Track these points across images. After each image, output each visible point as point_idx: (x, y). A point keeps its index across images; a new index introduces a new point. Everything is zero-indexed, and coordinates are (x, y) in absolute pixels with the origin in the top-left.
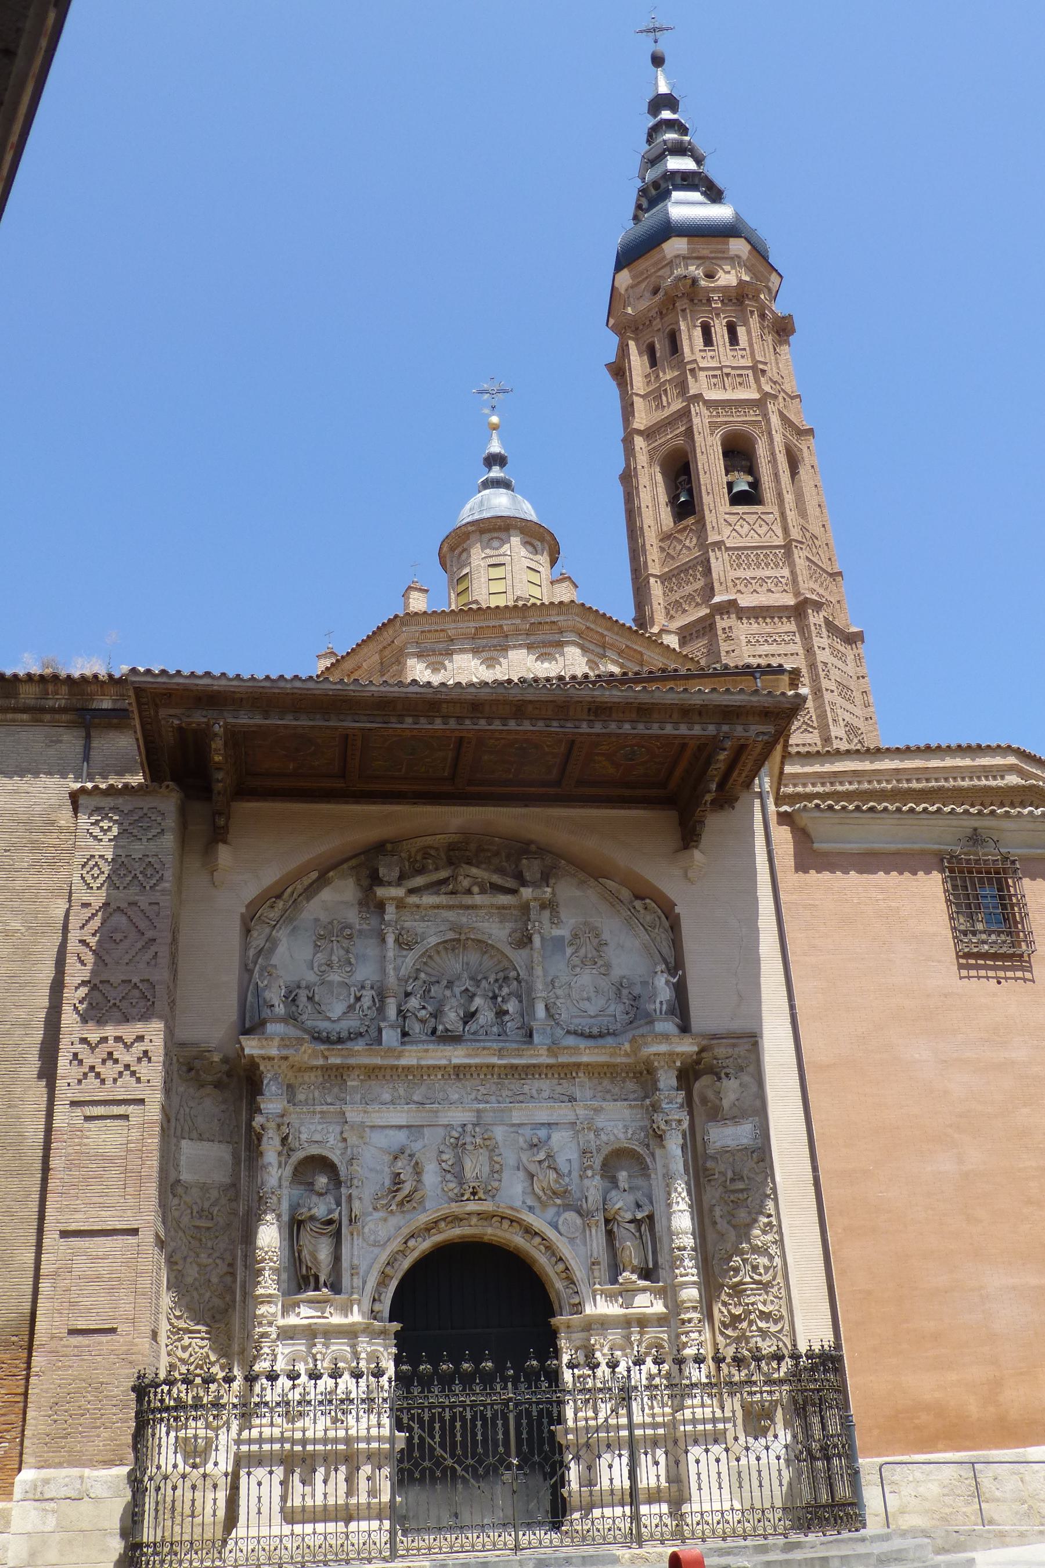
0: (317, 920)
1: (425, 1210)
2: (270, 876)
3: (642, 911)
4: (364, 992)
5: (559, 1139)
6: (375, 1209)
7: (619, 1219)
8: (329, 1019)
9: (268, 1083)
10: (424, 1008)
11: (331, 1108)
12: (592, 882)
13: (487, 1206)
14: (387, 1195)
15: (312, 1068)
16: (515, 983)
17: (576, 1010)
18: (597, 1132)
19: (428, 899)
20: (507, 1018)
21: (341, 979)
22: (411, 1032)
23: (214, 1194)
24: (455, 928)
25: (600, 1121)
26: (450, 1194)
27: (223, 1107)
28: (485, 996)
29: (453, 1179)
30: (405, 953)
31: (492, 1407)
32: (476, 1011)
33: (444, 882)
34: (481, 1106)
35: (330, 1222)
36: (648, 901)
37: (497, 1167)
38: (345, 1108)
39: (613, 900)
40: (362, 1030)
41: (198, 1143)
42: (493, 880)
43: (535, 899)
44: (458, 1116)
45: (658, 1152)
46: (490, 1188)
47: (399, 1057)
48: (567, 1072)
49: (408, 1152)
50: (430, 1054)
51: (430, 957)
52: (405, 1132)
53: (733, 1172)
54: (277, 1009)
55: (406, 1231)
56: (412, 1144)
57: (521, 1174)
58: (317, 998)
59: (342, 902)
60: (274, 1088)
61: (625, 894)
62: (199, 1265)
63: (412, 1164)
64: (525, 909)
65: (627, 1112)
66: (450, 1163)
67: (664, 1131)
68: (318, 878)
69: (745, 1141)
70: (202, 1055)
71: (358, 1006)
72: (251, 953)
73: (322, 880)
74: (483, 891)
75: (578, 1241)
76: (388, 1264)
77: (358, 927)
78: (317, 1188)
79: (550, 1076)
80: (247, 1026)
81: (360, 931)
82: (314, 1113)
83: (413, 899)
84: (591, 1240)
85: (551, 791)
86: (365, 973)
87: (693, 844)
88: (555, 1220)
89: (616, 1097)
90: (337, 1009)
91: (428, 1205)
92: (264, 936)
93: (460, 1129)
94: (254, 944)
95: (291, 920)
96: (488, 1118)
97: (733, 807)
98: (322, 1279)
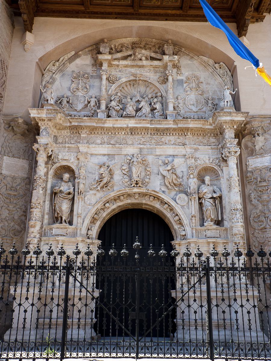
1: (114, 190)
2: (50, 47)
3: (219, 69)
4: (92, 99)
5: (177, 161)
6: (91, 189)
7: (205, 197)
8: (76, 110)
9: (42, 132)
10: (118, 106)
11: (73, 146)
12: (196, 57)
13: (143, 190)
14: (97, 183)
15: (65, 128)
16: (160, 98)
17: (188, 109)
18: (196, 159)
20: (155, 111)
21: (82, 95)
22: (111, 115)
23: (18, 181)
24: (134, 75)
25: (197, 155)
26: (126, 184)
27: (25, 145)
28: (146, 102)
29: (127, 177)
30: (111, 85)
32: (142, 107)
33: (130, 56)
34: (142, 146)
35: (69, 194)
36: (221, 63)
37: (148, 173)
38: (79, 145)
39: (205, 65)
41: (12, 158)
43: (170, 61)
44: (131, 150)
45: (224, 169)
46: (145, 182)
47: (104, 123)
48: (184, 131)
49: (107, 165)
50: (118, 122)
51: (123, 88)
52: (106, 157)
53: (261, 178)
55: (105, 199)
56: (109, 162)
57: (160, 177)
58: (71, 102)
59: (85, 64)
60: (44, 133)
61: (211, 62)
62: (9, 210)
63: (108, 170)
64: (165, 67)
65: (210, 151)
66: (126, 170)
67: (228, 157)
68: (75, 54)
69: (267, 164)
70: (14, 120)
71: (89, 105)
73: (76, 56)
74: (147, 59)
75: (185, 207)
76: (96, 214)
78: (64, 179)
79: (174, 134)
81: (92, 76)
82: (65, 147)
83: (116, 63)
84: (191, 206)
85: (178, 12)
86: (93, 92)
87: (244, 32)
88: (175, 197)
89: (205, 145)
90: (80, 106)
91: (115, 188)
92: (49, 77)
93: (131, 156)
94: (45, 80)
96: (145, 152)
97: (262, 21)
98: (64, 218)
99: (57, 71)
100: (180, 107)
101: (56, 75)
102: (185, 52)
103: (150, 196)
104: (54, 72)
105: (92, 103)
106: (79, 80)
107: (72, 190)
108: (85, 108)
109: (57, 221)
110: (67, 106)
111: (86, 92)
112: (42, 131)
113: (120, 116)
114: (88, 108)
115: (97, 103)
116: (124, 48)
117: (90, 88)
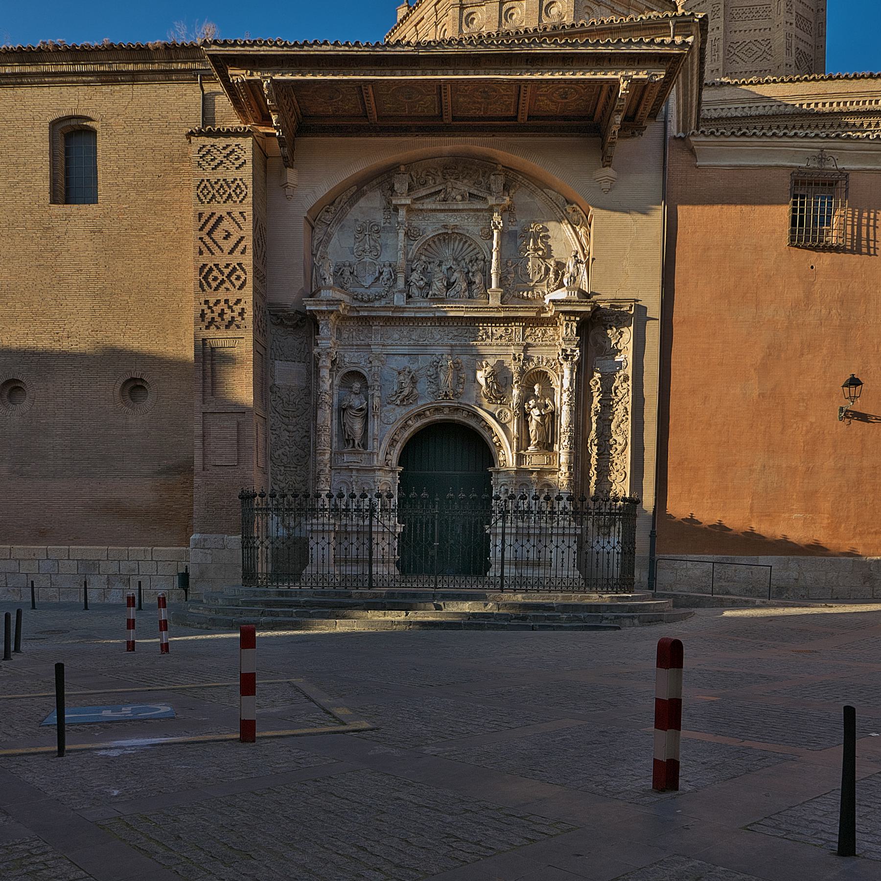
0: (357, 220)
4: (385, 269)
6: (389, 403)
10: (422, 279)
19: (428, 205)
20: (474, 287)
30: (412, 242)
31: (426, 517)
35: (361, 410)
36: (574, 206)
40: (383, 294)
42: (471, 191)
51: (429, 245)
54: (327, 281)
58: (355, 273)
68: (357, 191)
72: (316, 242)
77: (382, 225)
80: (313, 290)
83: (418, 206)
90: (369, 280)
95: (340, 220)
98: (356, 442)
99: (333, 222)
100: (510, 278)
101: (331, 228)
102: (523, 182)
103: (463, 410)
104: (329, 223)
105: (385, 276)
106: (366, 235)
107: (364, 405)
108: (376, 282)
109: (349, 444)
110: (351, 279)
111: (376, 256)
112: (323, 327)
113: (425, 295)
114: (380, 282)
115: (393, 275)
116: (430, 178)
117: (381, 250)
